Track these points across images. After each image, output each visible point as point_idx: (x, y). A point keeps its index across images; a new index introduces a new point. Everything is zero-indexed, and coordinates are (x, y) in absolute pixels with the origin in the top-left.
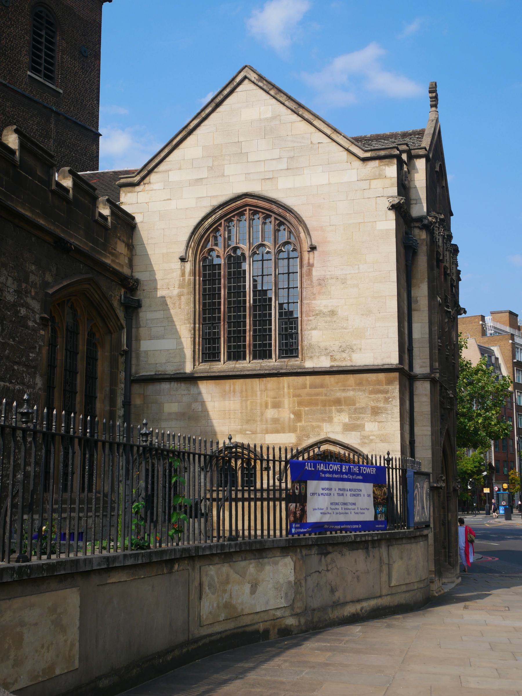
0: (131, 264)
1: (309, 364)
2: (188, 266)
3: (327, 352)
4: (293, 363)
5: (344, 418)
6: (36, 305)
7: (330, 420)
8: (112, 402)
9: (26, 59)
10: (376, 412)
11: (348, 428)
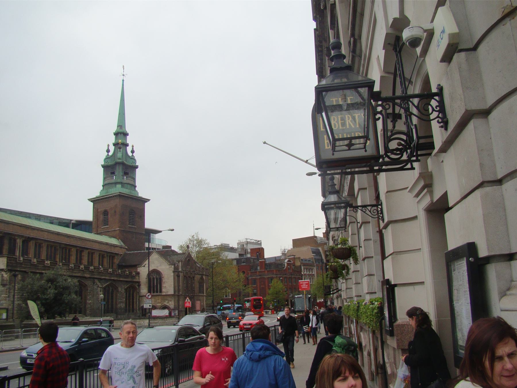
0: (139, 279)
1: (163, 294)
2: (147, 280)
3: (165, 292)
4: (160, 294)
5: (167, 302)
6: (123, 290)
7: (165, 302)
8: (136, 300)
9: (128, 223)
10: (171, 301)
11: (168, 303)
